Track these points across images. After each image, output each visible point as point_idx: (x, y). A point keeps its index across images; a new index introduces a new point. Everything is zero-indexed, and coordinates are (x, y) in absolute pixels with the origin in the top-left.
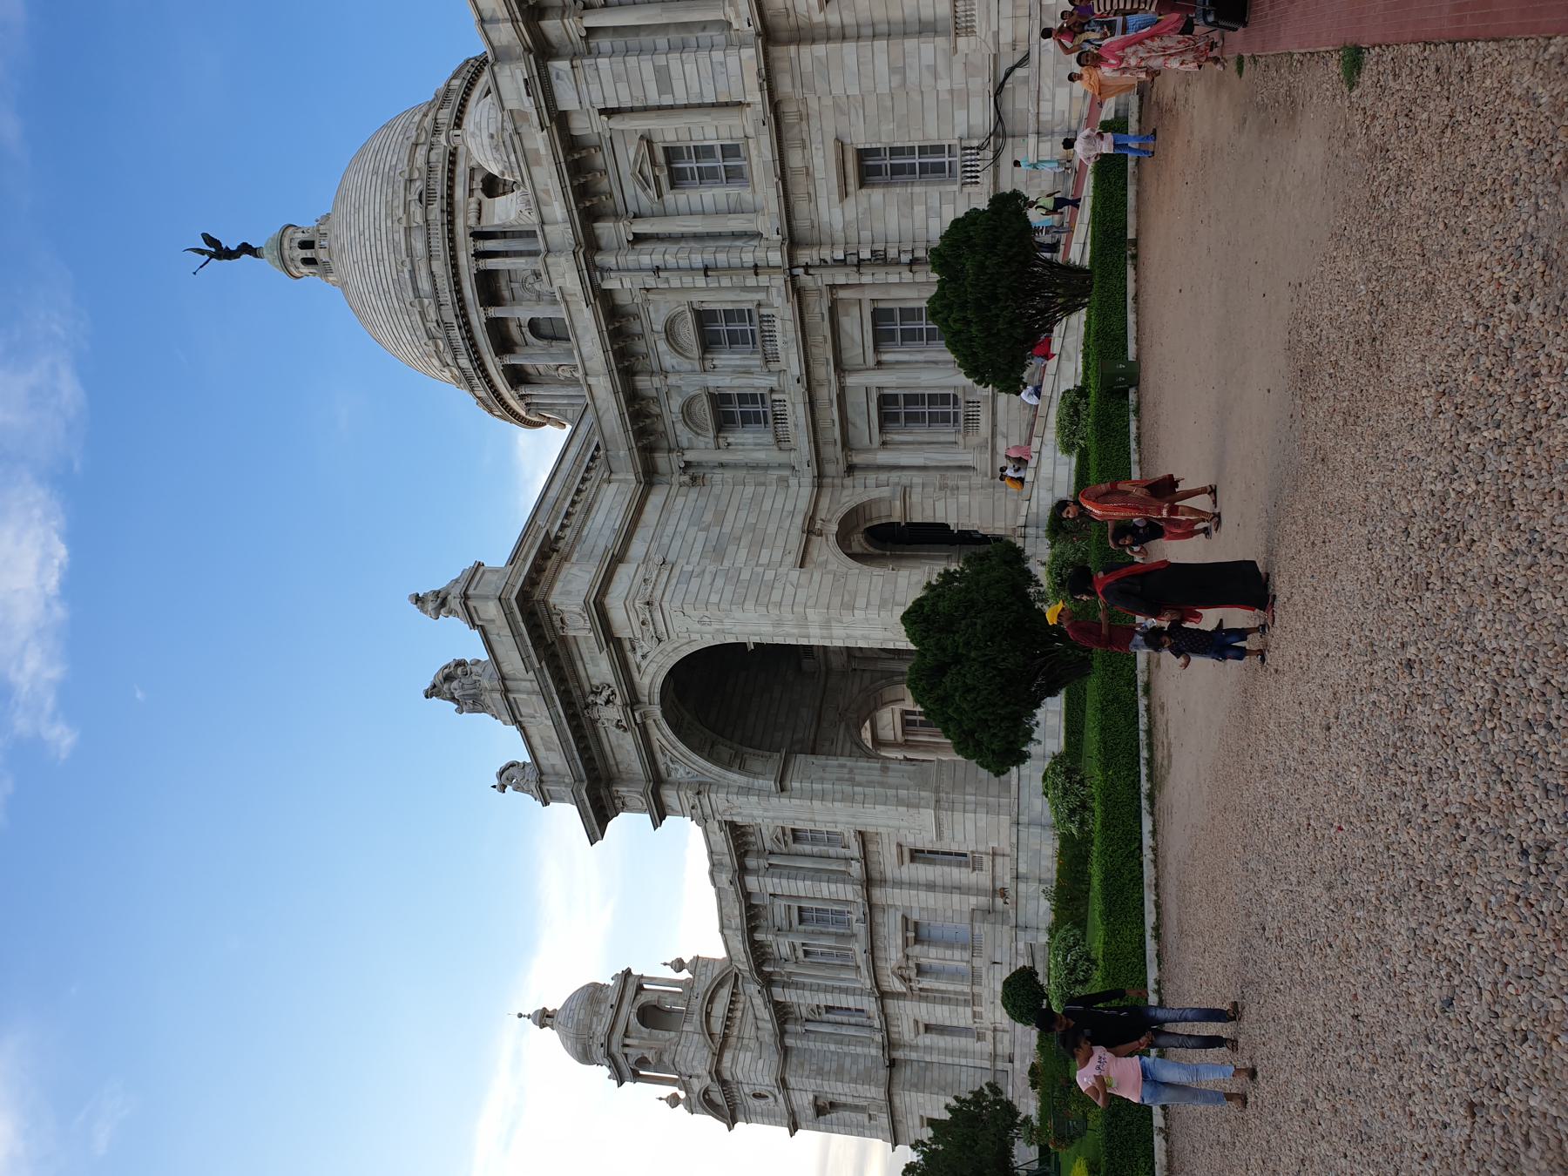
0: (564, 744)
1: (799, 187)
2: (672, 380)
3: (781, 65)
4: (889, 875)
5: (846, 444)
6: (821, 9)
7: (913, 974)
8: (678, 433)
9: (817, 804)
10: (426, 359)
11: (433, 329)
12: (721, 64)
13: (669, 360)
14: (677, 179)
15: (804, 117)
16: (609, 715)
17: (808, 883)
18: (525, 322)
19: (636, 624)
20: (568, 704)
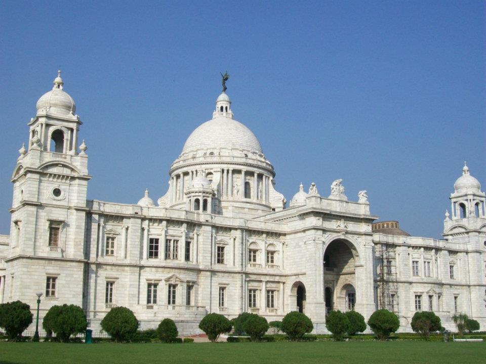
4: (213, 278)
7: (173, 282)
17: (210, 249)
19: (368, 242)
20: (347, 217)
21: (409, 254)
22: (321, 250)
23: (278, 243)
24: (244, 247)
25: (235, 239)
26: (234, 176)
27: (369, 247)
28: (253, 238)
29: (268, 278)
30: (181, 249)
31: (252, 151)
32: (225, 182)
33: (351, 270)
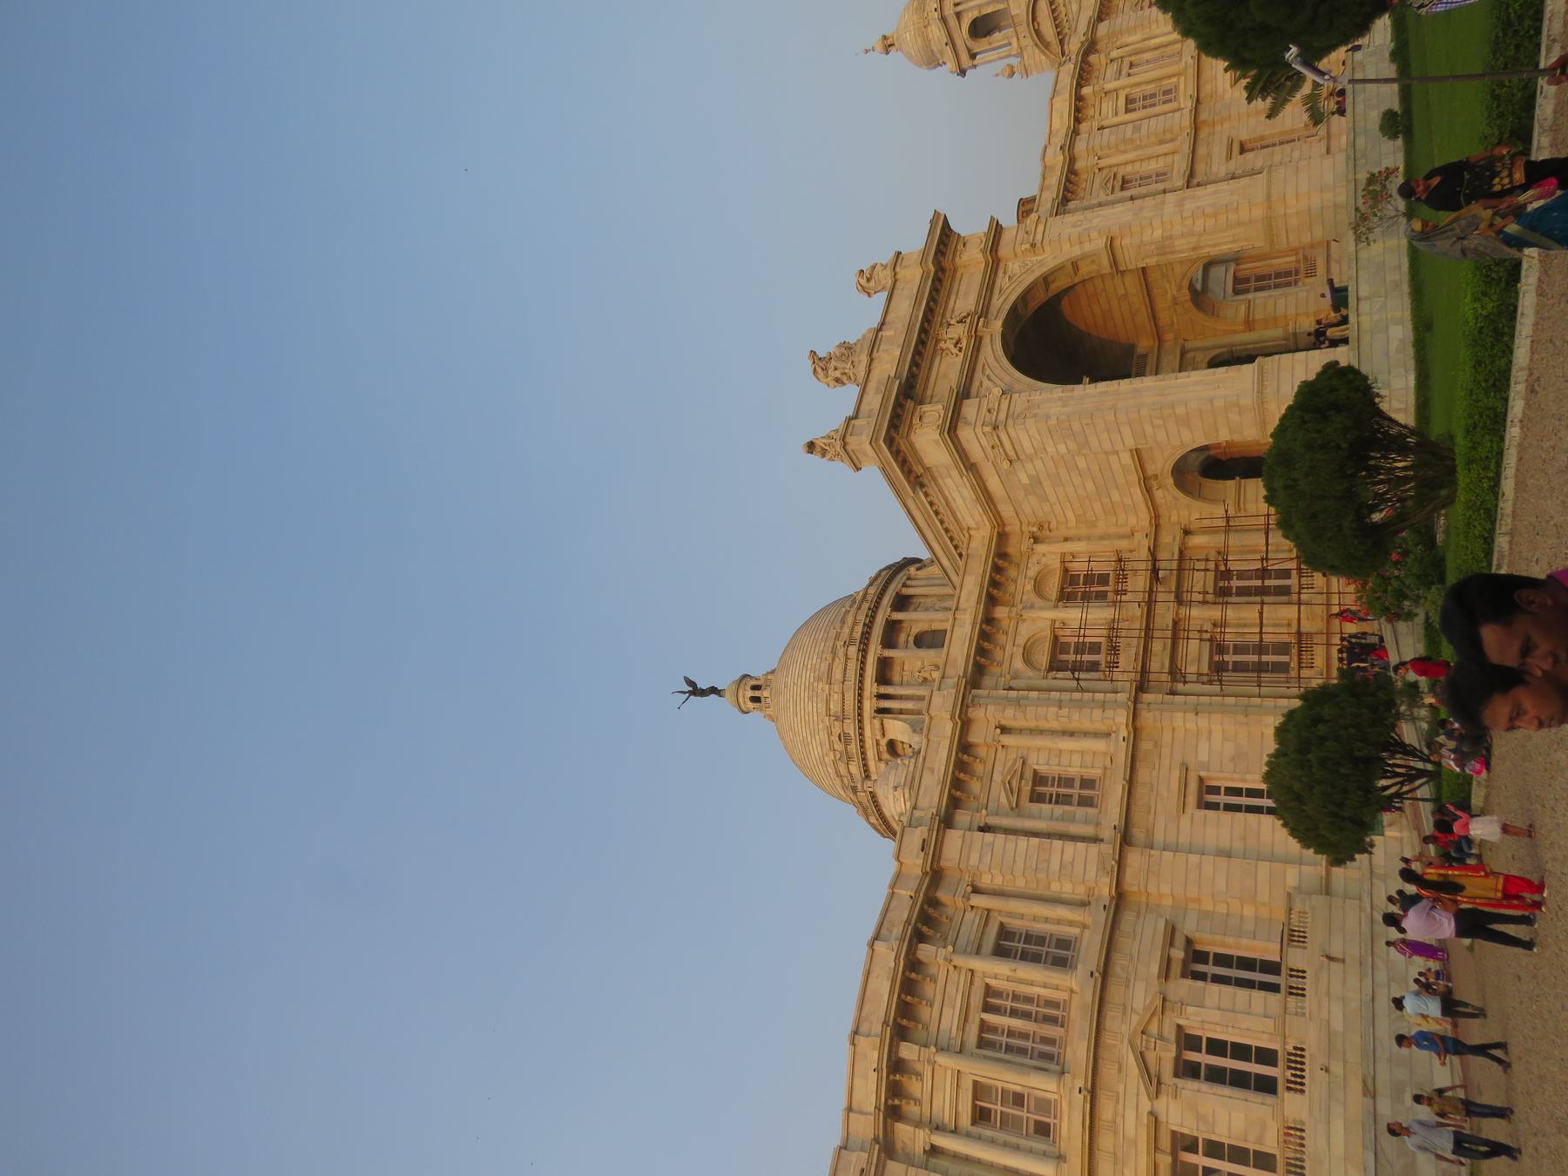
4: (1159, 837)
6: (1232, 87)
7: (1166, 1055)
10: (816, 684)
11: (838, 647)
16: (958, 331)
17: (1035, 841)
18: (915, 631)
21: (1101, 128)
22: (1036, 397)
23: (1034, 559)
24: (1034, 694)
25: (1004, 730)
26: (896, 679)
27: (1041, 228)
28: (1009, 655)
29: (1164, 596)
30: (1022, 982)
31: (838, 625)
32: (909, 705)
33: (1132, 285)
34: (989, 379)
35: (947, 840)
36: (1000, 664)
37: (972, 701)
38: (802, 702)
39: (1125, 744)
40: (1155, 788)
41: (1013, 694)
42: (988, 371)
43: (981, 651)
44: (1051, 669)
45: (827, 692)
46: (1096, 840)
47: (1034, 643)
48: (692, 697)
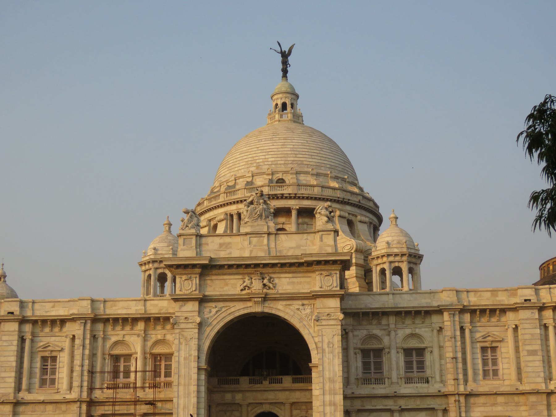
0: (242, 258)
1: (491, 399)
2: (393, 333)
3: (540, 397)
5: (359, 411)
8: (362, 331)
9: (195, 388)
10: (255, 165)
11: (277, 175)
12: (539, 375)
13: (402, 333)
14: (484, 349)
15: (517, 404)
16: (257, 285)
17: (14, 364)
19: (328, 311)
20: (265, 265)
21: (546, 327)
22: (194, 344)
34: (217, 312)
35: (14, 323)
36: (113, 329)
37: (81, 323)
38: (245, 157)
39: (62, 398)
40: (43, 413)
41: (87, 342)
42: (224, 309)
43: (116, 320)
44: (112, 356)
45: (247, 176)
46: (18, 389)
47: (125, 344)
48: (280, 55)
